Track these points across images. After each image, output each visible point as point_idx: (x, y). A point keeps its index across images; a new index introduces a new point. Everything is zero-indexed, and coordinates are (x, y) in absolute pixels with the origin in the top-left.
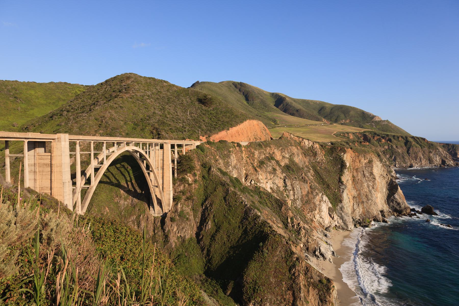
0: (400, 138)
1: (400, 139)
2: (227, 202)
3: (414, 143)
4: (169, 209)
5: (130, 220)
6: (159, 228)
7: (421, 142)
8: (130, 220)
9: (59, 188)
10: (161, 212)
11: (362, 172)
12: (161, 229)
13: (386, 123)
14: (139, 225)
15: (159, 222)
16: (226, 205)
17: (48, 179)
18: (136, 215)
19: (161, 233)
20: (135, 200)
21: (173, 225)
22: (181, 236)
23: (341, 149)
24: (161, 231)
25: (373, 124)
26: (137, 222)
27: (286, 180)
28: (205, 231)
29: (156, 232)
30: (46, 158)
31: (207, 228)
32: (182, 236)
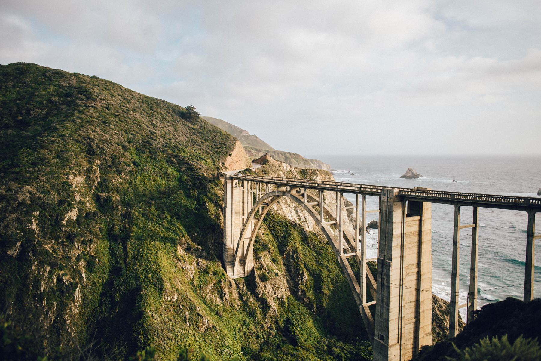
0: (280, 154)
1: (280, 155)
2: (312, 246)
3: (292, 159)
4: (251, 266)
5: (208, 291)
6: (246, 293)
7: (297, 158)
8: (208, 291)
9: (428, 262)
10: (242, 272)
11: (330, 195)
12: (251, 294)
13: (255, 138)
14: (222, 295)
15: (245, 287)
16: (311, 249)
17: (414, 253)
18: (213, 282)
19: (252, 300)
20: (203, 262)
21: (267, 286)
22: (277, 297)
23: (312, 172)
24: (252, 297)
25: (243, 138)
26: (218, 291)
27: (298, 211)
28: (303, 284)
29: (245, 298)
30: (413, 224)
31: (305, 281)
32: (279, 297)
